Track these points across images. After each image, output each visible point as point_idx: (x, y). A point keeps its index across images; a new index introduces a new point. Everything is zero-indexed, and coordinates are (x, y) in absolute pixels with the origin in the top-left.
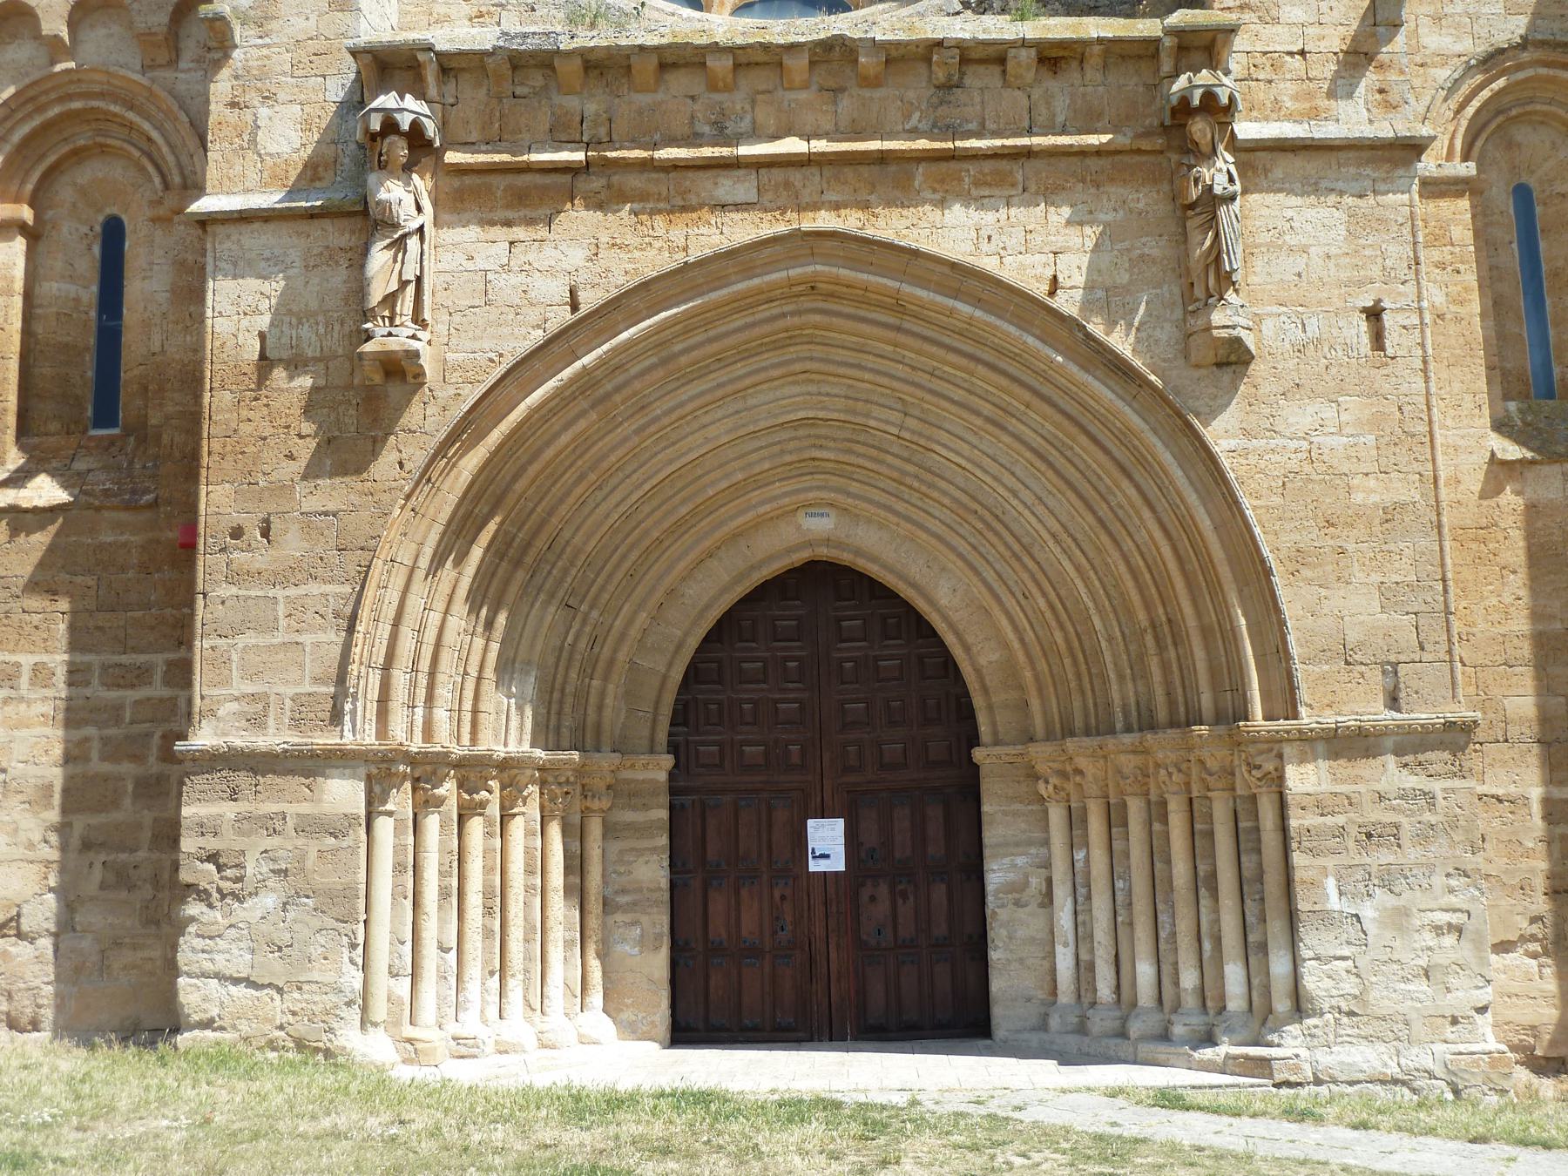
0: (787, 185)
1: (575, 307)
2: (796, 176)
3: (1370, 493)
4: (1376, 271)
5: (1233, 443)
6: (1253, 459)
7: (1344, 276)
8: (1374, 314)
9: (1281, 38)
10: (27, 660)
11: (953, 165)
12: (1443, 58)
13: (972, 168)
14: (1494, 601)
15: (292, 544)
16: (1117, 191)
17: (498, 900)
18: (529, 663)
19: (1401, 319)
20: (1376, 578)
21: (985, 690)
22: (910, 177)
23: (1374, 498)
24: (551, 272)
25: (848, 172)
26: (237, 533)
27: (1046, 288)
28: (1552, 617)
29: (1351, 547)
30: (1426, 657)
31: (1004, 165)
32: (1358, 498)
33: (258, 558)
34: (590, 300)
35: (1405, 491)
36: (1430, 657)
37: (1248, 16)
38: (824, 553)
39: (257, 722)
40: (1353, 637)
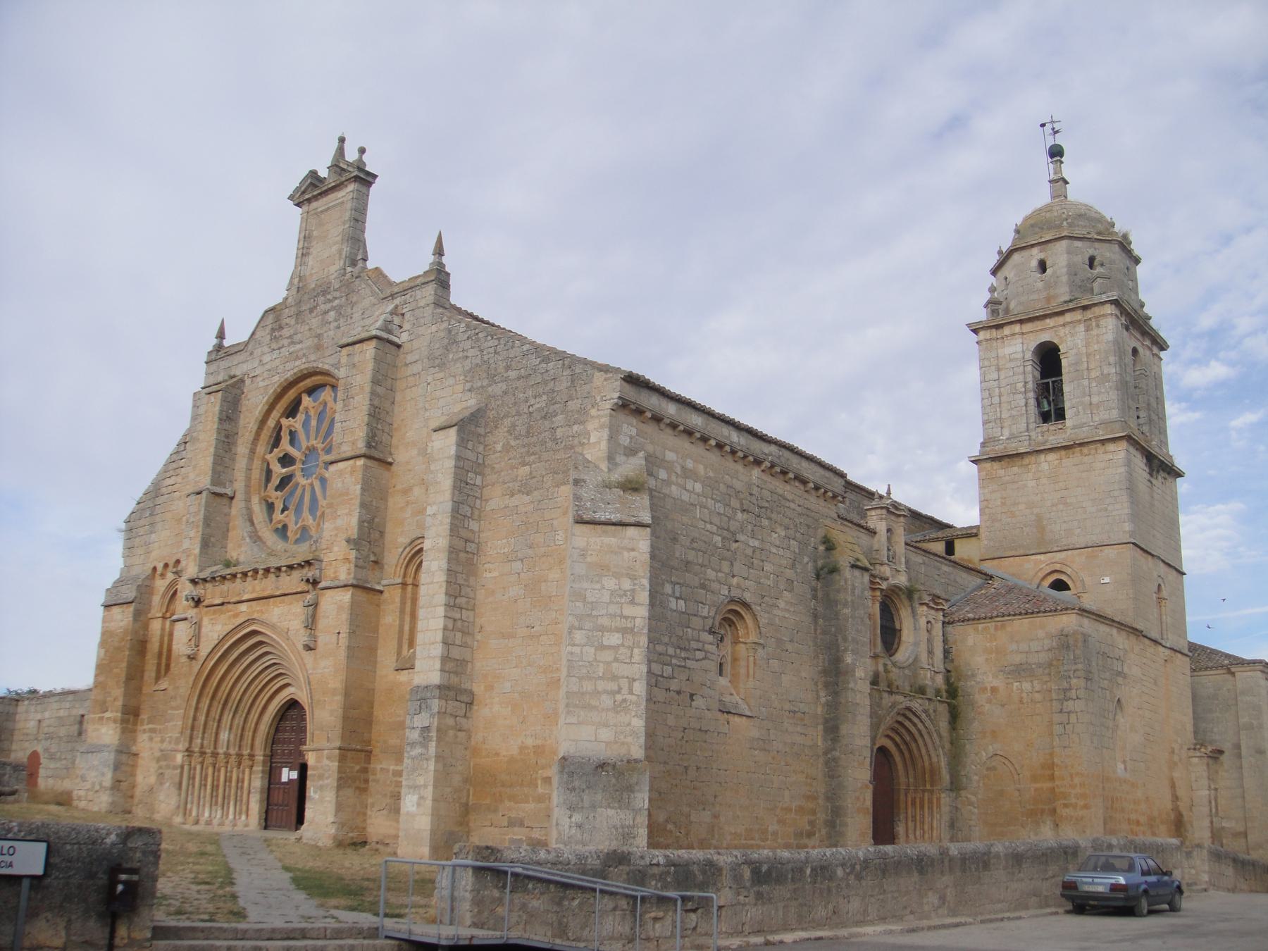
9: (331, 557)
17: (215, 787)
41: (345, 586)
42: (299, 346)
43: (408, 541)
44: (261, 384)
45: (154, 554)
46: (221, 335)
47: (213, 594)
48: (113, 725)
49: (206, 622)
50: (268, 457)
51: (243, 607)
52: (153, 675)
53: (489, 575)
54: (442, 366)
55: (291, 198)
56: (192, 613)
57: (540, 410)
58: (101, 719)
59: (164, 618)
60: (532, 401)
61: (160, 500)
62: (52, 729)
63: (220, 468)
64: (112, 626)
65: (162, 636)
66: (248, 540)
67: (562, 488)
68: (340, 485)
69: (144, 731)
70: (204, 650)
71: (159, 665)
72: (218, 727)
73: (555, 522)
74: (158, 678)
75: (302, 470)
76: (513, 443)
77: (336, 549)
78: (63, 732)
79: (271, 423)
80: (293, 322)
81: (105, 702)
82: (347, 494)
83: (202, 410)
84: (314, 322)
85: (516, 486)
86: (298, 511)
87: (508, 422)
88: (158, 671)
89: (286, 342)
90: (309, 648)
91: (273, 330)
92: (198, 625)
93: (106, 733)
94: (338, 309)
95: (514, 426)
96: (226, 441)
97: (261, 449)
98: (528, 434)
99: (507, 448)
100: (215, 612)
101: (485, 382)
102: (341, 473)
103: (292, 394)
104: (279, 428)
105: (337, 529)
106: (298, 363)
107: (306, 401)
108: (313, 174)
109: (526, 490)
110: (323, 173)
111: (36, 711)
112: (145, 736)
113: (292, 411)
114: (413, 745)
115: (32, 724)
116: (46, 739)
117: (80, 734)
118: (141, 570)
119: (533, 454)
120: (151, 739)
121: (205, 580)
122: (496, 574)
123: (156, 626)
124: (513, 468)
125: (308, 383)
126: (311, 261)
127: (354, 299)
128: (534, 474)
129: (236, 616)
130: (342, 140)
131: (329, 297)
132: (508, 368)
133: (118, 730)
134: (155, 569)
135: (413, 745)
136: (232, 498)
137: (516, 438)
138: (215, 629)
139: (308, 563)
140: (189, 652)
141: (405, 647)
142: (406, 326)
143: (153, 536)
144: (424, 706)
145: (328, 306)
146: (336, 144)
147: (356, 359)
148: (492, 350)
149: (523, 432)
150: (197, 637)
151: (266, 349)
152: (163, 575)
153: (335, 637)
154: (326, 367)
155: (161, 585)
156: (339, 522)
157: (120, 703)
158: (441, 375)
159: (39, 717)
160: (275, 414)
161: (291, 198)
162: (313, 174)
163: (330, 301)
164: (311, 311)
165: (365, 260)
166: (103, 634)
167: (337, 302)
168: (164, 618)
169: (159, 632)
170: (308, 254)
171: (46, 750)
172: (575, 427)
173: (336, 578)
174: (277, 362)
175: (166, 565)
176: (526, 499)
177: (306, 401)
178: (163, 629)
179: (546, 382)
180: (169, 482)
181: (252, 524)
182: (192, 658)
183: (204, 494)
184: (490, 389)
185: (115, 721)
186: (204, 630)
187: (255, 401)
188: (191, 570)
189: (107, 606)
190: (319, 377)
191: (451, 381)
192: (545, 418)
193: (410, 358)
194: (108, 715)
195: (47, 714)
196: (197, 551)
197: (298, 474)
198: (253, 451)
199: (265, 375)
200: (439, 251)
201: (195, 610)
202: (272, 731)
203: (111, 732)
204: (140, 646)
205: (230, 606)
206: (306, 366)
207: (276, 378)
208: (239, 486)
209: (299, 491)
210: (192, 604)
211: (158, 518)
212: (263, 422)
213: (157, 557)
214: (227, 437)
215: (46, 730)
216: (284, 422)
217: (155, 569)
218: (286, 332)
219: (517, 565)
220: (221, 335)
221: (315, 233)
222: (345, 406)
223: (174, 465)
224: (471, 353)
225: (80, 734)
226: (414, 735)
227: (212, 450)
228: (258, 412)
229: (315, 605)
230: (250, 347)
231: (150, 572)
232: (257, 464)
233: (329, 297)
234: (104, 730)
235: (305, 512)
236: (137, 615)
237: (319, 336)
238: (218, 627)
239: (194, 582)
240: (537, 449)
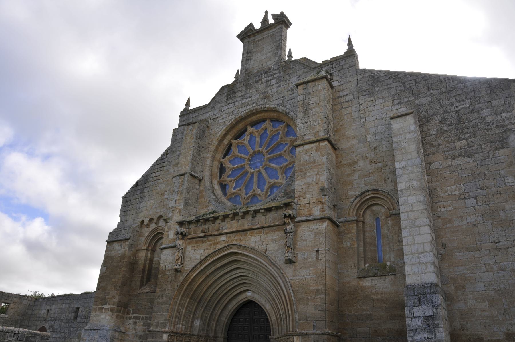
0: (230, 237)
1: (201, 259)
2: (231, 235)
3: (313, 287)
4: (318, 243)
5: (291, 278)
6: (294, 281)
7: (312, 245)
8: (317, 251)
9: (305, 201)
10: (141, 316)
11: (252, 231)
12: (352, 196)
13: (256, 231)
14: (356, 307)
15: (165, 299)
16: (277, 233)
18: (198, 318)
19: (322, 252)
20: (313, 304)
21: (272, 325)
22: (247, 233)
23: (314, 288)
24: (198, 254)
25: (238, 234)
26: (159, 297)
27: (264, 251)
28: (368, 310)
29: (309, 297)
30: (321, 319)
31: (260, 230)
32: (312, 288)
33: (160, 301)
34: (203, 258)
35: (321, 287)
36: (321, 319)
37: (301, 198)
38: (249, 299)
39: (157, 327)
40: (308, 315)
41: (322, 218)
42: (248, 100)
43: (357, 193)
44: (221, 121)
45: (141, 215)
46: (188, 104)
47: (198, 231)
48: (110, 313)
49: (189, 248)
50: (223, 160)
51: (223, 238)
52: (138, 283)
53: (443, 209)
54: (370, 94)
55: (238, 36)
56: (179, 243)
57: (465, 108)
58: (100, 309)
59: (147, 250)
60: (458, 104)
61: (146, 185)
62: (56, 315)
63: (195, 163)
64: (113, 253)
65: (145, 261)
66: (213, 203)
67: (502, 150)
68: (307, 158)
69: (130, 318)
70: (189, 266)
71: (143, 277)
72: (193, 317)
73: (502, 172)
74: (141, 286)
75: (250, 165)
76: (446, 128)
77: (308, 196)
78: (63, 317)
79: (226, 142)
80: (243, 89)
81: (105, 299)
82: (315, 162)
83: (177, 138)
84: (260, 87)
85: (456, 153)
86: (248, 186)
87: (439, 117)
88: (142, 281)
89: (239, 99)
90: (290, 261)
91: (228, 95)
92: (184, 250)
93: (104, 319)
94: (279, 79)
95: (444, 119)
96: (199, 150)
97: (219, 156)
98: (459, 122)
99: (441, 132)
100: (196, 242)
101: (411, 99)
102: (307, 151)
103: (241, 126)
104: (230, 146)
105: (308, 184)
106: (248, 107)
107: (250, 129)
108: (251, 25)
109: (464, 153)
110: (258, 26)
111: (46, 304)
112: (131, 321)
113: (238, 136)
114: (416, 331)
115: (43, 312)
116: (52, 320)
117: (76, 318)
118: (134, 222)
119: (467, 133)
120: (135, 323)
121: (190, 223)
122: (451, 208)
123: (142, 255)
124: (450, 143)
125: (254, 118)
126: (252, 62)
127: (291, 72)
128: (471, 144)
129: (217, 243)
130: (266, 12)
131: (271, 73)
132: (429, 90)
133: (114, 317)
134: (143, 222)
135: (416, 331)
136: (200, 180)
137: (448, 126)
138: (195, 254)
139: (287, 205)
140: (177, 267)
141: (362, 262)
142: (335, 78)
143: (142, 204)
144: (422, 299)
145: (270, 78)
146: (264, 14)
147: (310, 90)
148: (413, 82)
149: (454, 120)
150: (182, 259)
151: (223, 104)
152: (148, 226)
153: (315, 253)
154: (273, 106)
155: (147, 231)
156: (309, 180)
157: (116, 299)
158: (372, 98)
159: (48, 307)
160: (229, 137)
161: (238, 36)
162: (251, 25)
163: (271, 75)
164: (257, 82)
165: (292, 57)
166: (105, 258)
167: (276, 75)
168: (147, 250)
169: (143, 258)
170: (250, 59)
171: (51, 327)
172: (504, 115)
173: (310, 215)
174: (233, 109)
175: (151, 220)
176: (469, 160)
177: (250, 129)
178: (146, 256)
179: (467, 93)
180: (154, 175)
181: (215, 195)
182: (177, 271)
183: (187, 175)
184: (417, 102)
185: (112, 310)
186: (187, 253)
187: (218, 130)
188: (177, 218)
189: (109, 242)
190: (263, 114)
191: (381, 101)
192: (472, 111)
193: (341, 94)
194: (105, 307)
195: (54, 306)
196: (181, 207)
197: (247, 167)
198: (214, 157)
199: (223, 116)
200: (350, 43)
201: (181, 241)
202: (230, 322)
203: (108, 317)
204: (133, 265)
205: (210, 238)
206: (256, 107)
207: (233, 116)
208: (207, 174)
209: (249, 176)
210: (180, 236)
211: (146, 194)
212: (221, 141)
213: (145, 215)
214: (199, 147)
215: (52, 315)
216: (233, 141)
217: (143, 222)
218: (239, 94)
219: (472, 202)
220: (188, 104)
221: (254, 50)
222: (305, 115)
223: (159, 166)
224: (394, 85)
225: (76, 318)
226: (418, 323)
227: (191, 152)
228: (219, 135)
229: (295, 232)
230: (211, 105)
231: (139, 223)
232: (216, 164)
233: (271, 73)
234: (103, 316)
235: (255, 187)
236: (131, 246)
237: (265, 92)
238: (202, 251)
239: (181, 224)
240: (471, 130)
